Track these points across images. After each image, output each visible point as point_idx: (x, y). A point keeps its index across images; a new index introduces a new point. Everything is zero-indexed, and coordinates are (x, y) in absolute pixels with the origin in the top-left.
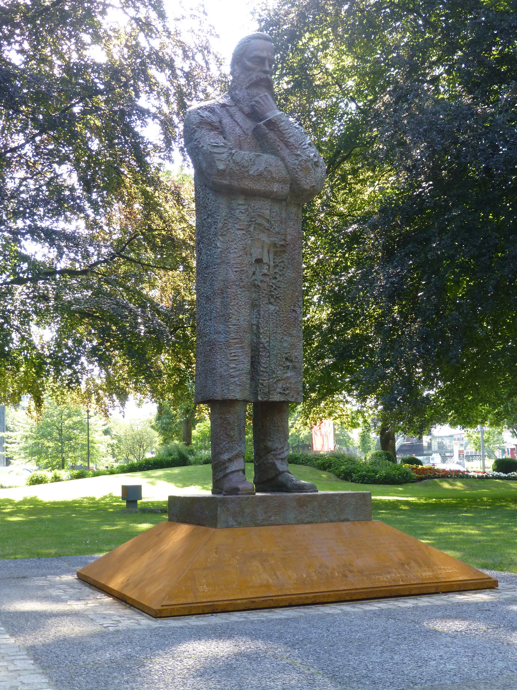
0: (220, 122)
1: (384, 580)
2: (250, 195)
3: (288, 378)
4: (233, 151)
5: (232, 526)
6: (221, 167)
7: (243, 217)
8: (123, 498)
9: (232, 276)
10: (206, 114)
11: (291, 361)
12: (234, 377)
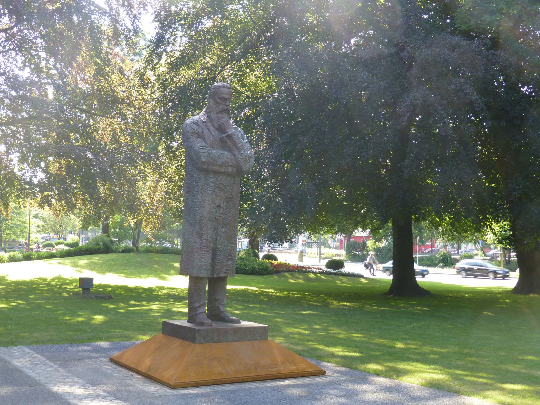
0: (203, 132)
1: (274, 371)
2: (216, 173)
3: (229, 265)
4: (210, 152)
5: (202, 343)
6: (204, 160)
8: (80, 287)
9: (205, 214)
10: (195, 127)
11: (231, 256)
12: (203, 266)
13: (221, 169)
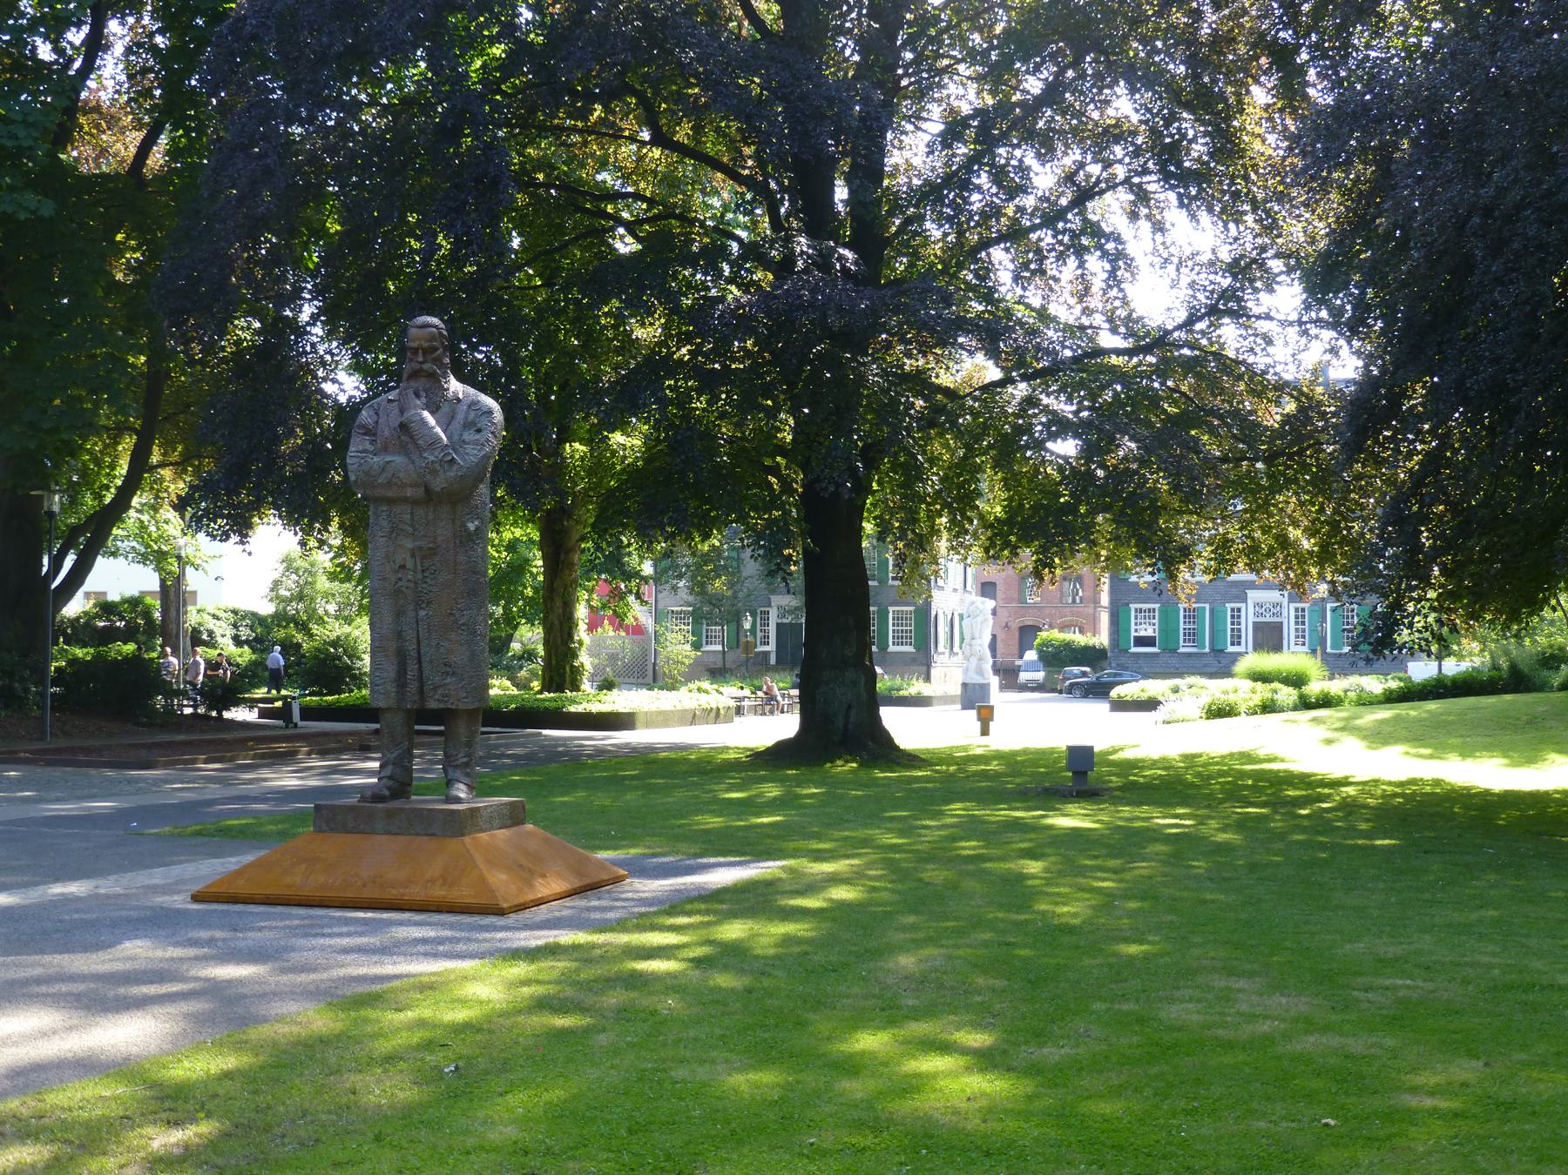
1: (392, 893)
2: (391, 502)
7: (385, 524)
13: (389, 494)
